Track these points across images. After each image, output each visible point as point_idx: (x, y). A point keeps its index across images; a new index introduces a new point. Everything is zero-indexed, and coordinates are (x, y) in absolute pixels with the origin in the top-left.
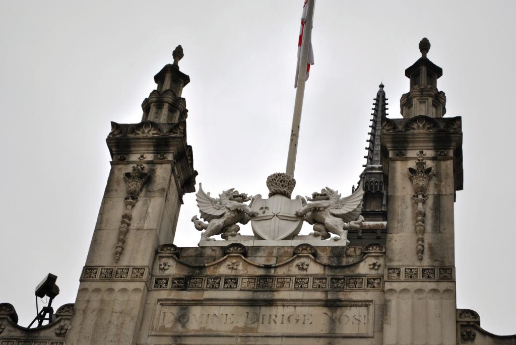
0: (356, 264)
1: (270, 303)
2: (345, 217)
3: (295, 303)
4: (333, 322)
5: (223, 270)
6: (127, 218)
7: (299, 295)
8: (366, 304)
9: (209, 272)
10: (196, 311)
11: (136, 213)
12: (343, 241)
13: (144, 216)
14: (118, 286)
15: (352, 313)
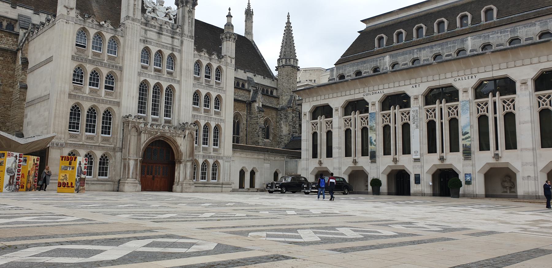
0: (176, 29)
1: (162, 34)
2: (174, 16)
3: (167, 35)
4: (173, 41)
5: (153, 23)
6: (135, 5)
7: (167, 34)
8: (178, 39)
9: (150, 23)
10: (148, 32)
11: (136, 3)
12: (173, 22)
13: (138, 5)
14: (135, 23)
15: (176, 40)
